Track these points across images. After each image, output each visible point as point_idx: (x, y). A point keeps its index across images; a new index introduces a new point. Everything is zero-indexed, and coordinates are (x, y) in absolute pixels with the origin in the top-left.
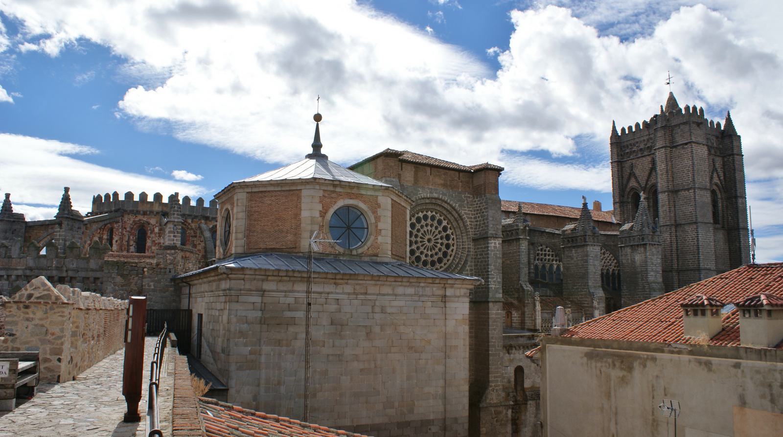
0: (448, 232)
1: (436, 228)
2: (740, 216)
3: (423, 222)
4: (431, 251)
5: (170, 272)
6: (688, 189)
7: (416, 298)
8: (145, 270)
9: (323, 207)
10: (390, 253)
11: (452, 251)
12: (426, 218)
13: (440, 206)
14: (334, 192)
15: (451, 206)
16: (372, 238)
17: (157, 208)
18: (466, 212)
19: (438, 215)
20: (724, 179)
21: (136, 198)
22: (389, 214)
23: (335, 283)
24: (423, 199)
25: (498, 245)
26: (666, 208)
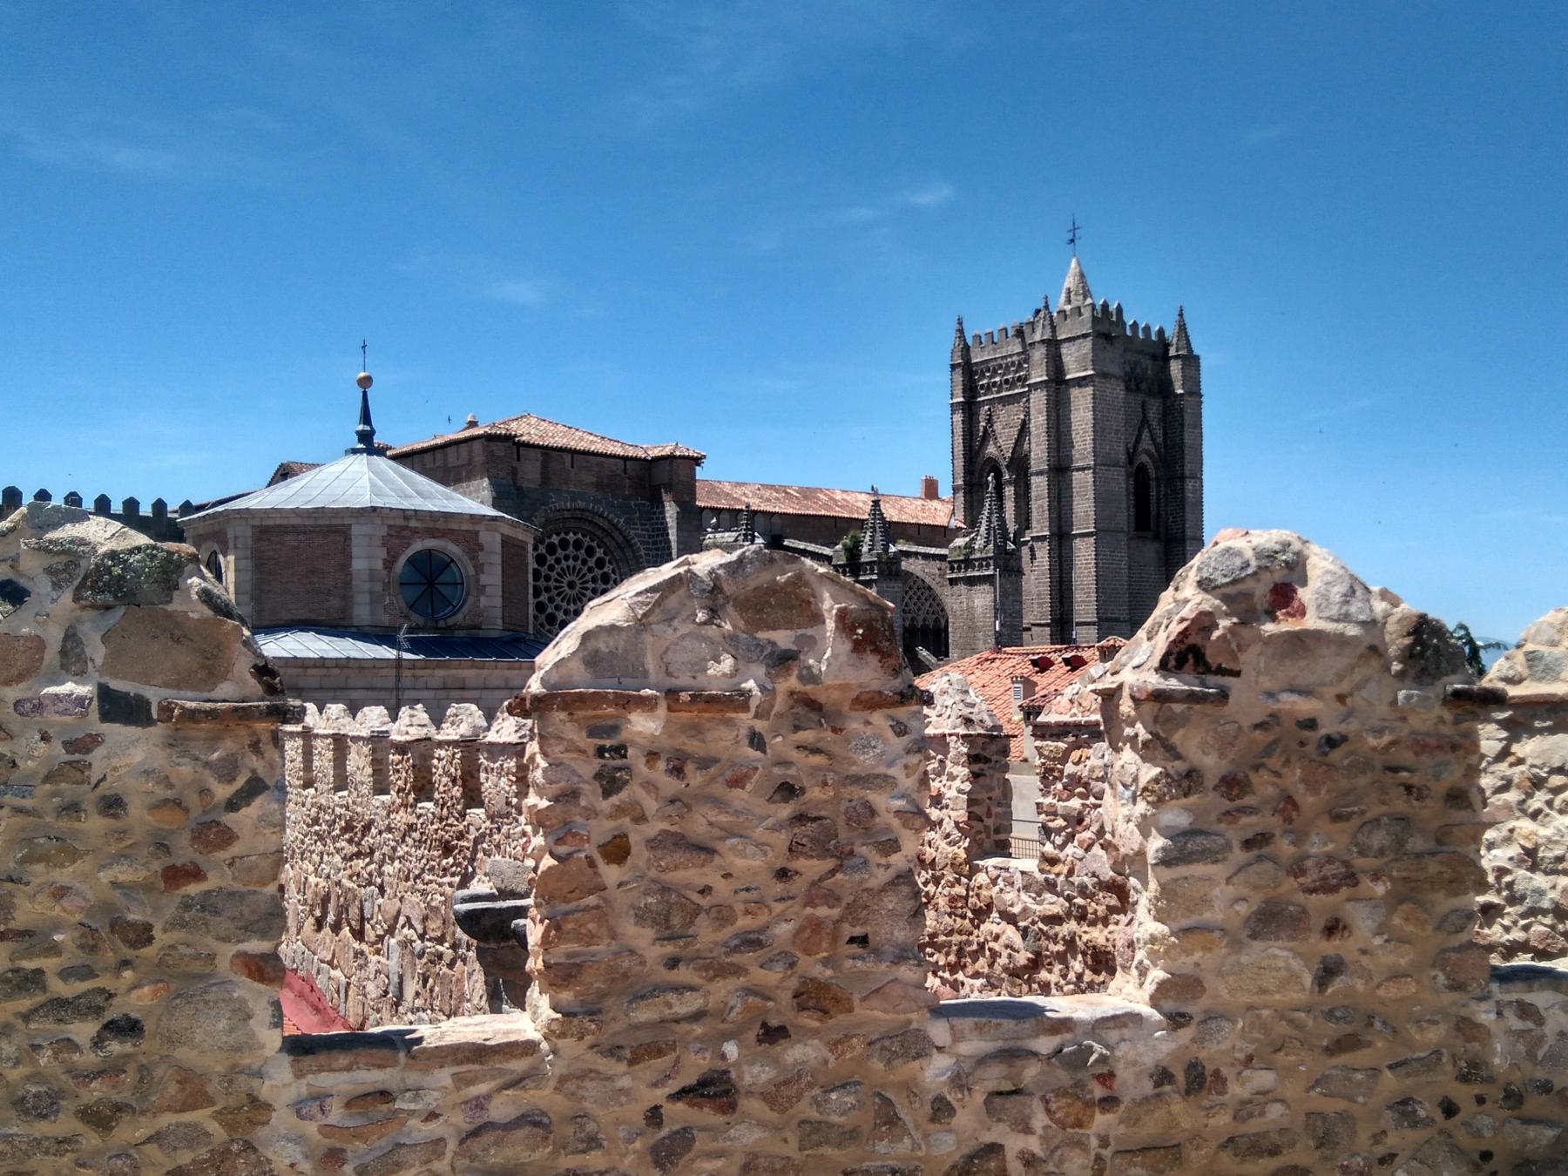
0: (606, 570)
1: (584, 562)
2: (1189, 516)
3: (560, 553)
6: (1083, 469)
10: (500, 622)
12: (564, 544)
13: (590, 522)
14: (406, 528)
15: (610, 522)
16: (471, 599)
20: (1165, 440)
22: (498, 559)
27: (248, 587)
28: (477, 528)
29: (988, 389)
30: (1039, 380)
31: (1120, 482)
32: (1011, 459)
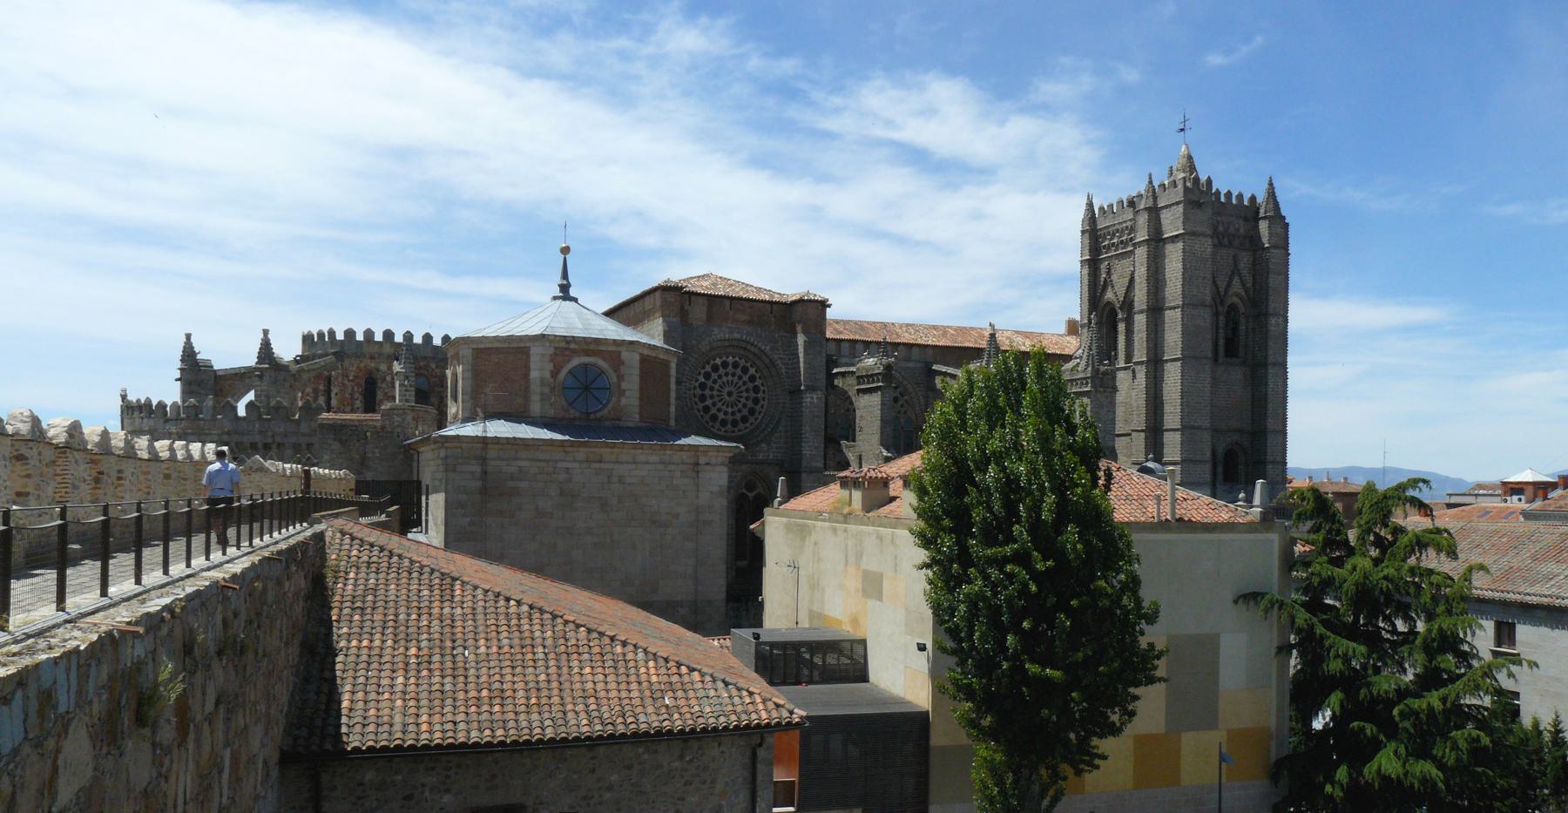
0: (756, 383)
1: (740, 378)
4: (732, 407)
5: (398, 436)
6: (1174, 308)
7: (661, 467)
8: (368, 434)
9: (554, 366)
10: (637, 416)
11: (762, 407)
12: (725, 365)
13: (745, 349)
14: (566, 349)
15: (760, 349)
16: (614, 399)
17: (388, 349)
18: (781, 356)
19: (743, 361)
21: (360, 337)
22: (636, 372)
23: (565, 452)
24: (721, 340)
25: (815, 401)
26: (1144, 335)
27: (469, 389)
28: (620, 349)
29: (1108, 248)
30: (1142, 239)
31: (1205, 318)
32: (1124, 302)
